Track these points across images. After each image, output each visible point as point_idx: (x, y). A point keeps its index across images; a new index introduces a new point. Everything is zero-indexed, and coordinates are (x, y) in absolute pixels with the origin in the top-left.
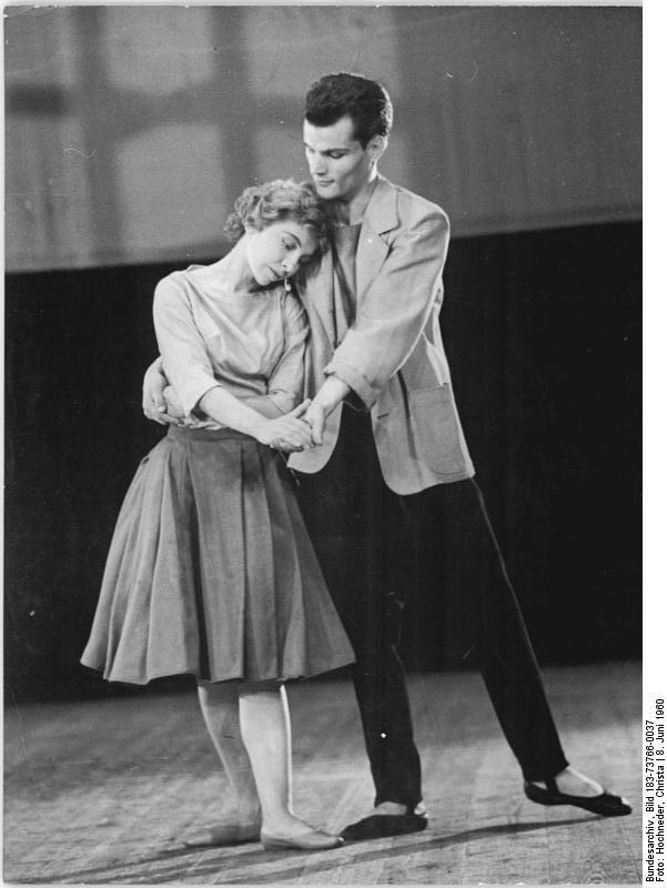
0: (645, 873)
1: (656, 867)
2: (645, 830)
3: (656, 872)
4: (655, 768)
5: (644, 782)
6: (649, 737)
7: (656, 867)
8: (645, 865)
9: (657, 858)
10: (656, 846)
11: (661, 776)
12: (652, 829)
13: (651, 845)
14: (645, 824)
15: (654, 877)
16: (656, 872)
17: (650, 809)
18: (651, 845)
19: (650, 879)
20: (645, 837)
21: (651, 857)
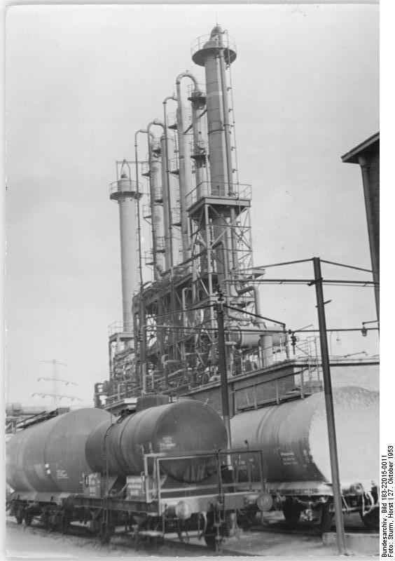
0: (381, 552)
1: (388, 548)
2: (381, 525)
3: (388, 551)
5: (381, 494)
7: (388, 548)
8: (381, 547)
9: (389, 541)
10: (388, 534)
12: (385, 523)
13: (385, 534)
14: (381, 521)
15: (387, 554)
16: (388, 551)
17: (384, 511)
18: (385, 534)
19: (384, 556)
20: (381, 529)
21: (385, 541)
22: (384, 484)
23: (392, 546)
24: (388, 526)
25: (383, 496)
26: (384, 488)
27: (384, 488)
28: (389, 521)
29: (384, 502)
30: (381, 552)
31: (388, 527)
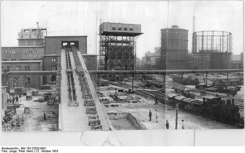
1: (6, 150)
3: (4, 150)
4: (32, 150)
6: (42, 148)
7: (6, 150)
9: (9, 150)
10: (12, 150)
11: (31, 151)
12: (16, 149)
13: (12, 149)
15: (3, 149)
16: (4, 150)
17: (22, 148)
18: (12, 149)
19: (2, 148)
21: (9, 148)
22: (34, 148)
23: (6, 151)
24: (15, 150)
25: (28, 148)
26: (32, 148)
27: (32, 148)
28: (18, 150)
29: (26, 148)
30: (4, 147)
31: (15, 150)
